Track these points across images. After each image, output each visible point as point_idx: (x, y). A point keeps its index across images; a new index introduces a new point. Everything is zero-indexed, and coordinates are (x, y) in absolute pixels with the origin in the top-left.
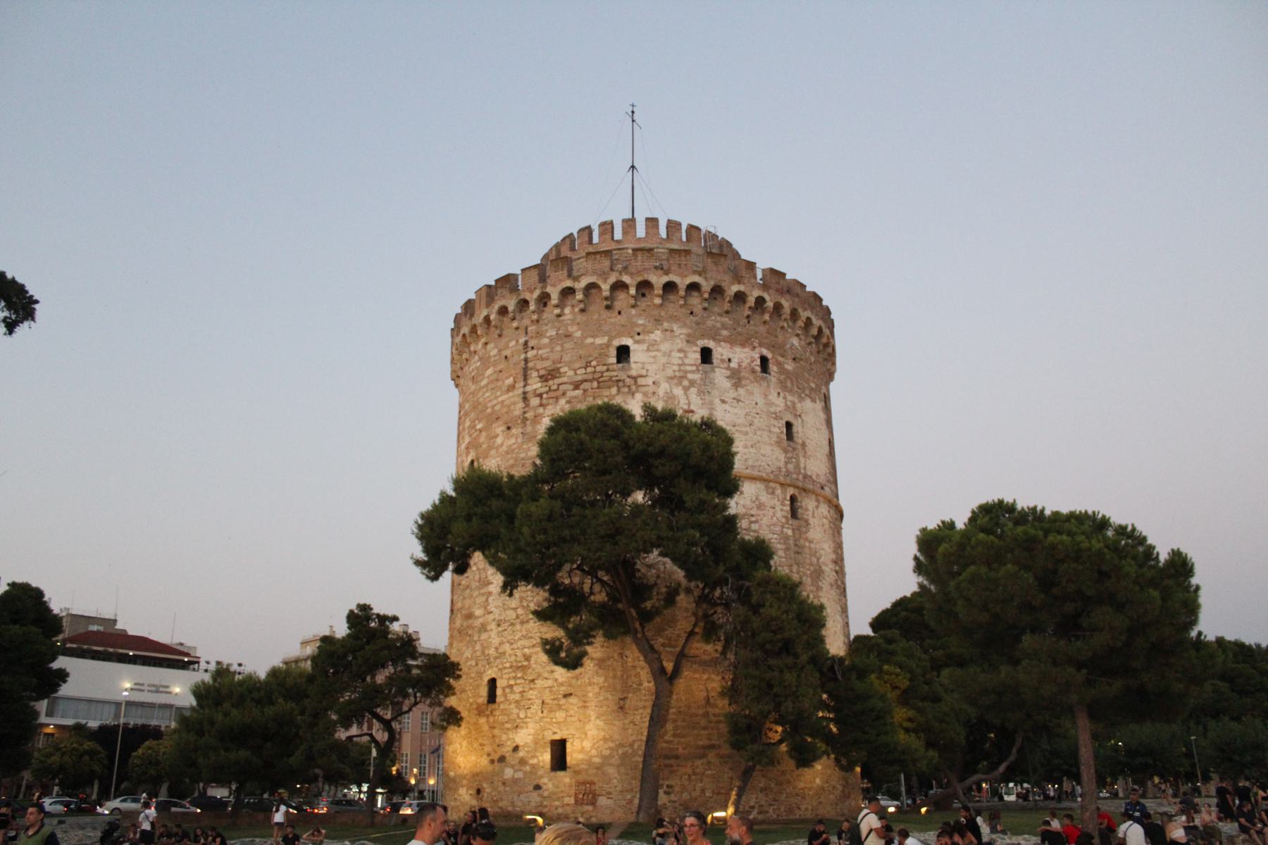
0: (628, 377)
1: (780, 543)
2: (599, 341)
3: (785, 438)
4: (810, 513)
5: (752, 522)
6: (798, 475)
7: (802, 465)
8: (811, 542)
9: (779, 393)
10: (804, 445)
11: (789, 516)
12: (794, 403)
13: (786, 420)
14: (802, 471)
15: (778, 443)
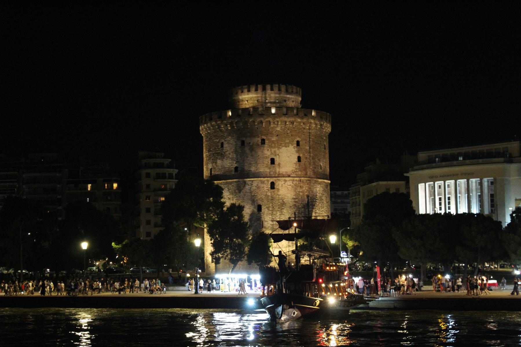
0: (224, 152)
1: (265, 198)
2: (217, 141)
3: (270, 164)
4: (280, 186)
5: (255, 193)
6: (275, 175)
7: (277, 171)
8: (279, 195)
9: (268, 150)
10: (279, 164)
11: (270, 189)
12: (275, 152)
13: (271, 158)
14: (278, 173)
15: (266, 167)
